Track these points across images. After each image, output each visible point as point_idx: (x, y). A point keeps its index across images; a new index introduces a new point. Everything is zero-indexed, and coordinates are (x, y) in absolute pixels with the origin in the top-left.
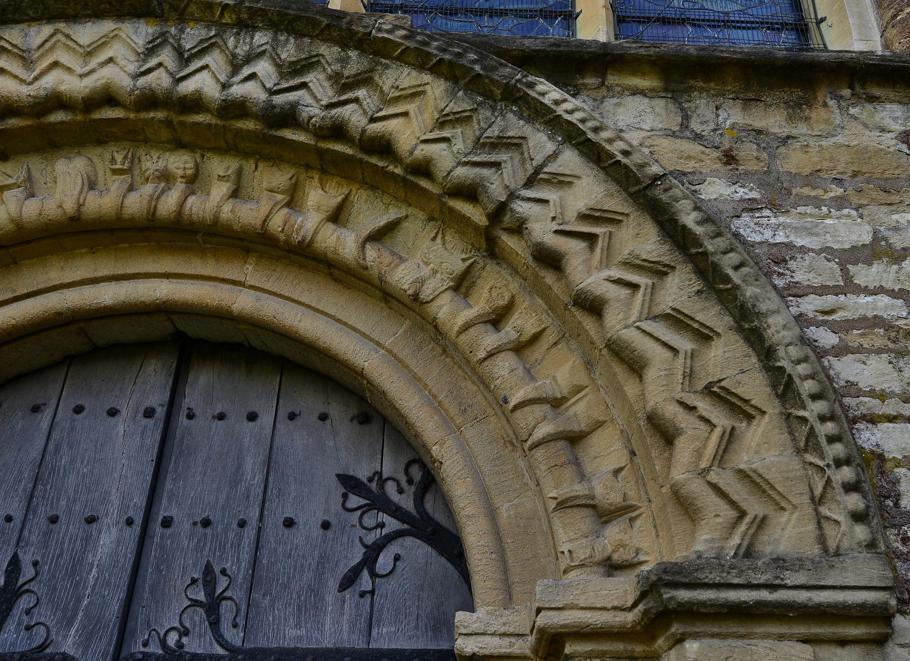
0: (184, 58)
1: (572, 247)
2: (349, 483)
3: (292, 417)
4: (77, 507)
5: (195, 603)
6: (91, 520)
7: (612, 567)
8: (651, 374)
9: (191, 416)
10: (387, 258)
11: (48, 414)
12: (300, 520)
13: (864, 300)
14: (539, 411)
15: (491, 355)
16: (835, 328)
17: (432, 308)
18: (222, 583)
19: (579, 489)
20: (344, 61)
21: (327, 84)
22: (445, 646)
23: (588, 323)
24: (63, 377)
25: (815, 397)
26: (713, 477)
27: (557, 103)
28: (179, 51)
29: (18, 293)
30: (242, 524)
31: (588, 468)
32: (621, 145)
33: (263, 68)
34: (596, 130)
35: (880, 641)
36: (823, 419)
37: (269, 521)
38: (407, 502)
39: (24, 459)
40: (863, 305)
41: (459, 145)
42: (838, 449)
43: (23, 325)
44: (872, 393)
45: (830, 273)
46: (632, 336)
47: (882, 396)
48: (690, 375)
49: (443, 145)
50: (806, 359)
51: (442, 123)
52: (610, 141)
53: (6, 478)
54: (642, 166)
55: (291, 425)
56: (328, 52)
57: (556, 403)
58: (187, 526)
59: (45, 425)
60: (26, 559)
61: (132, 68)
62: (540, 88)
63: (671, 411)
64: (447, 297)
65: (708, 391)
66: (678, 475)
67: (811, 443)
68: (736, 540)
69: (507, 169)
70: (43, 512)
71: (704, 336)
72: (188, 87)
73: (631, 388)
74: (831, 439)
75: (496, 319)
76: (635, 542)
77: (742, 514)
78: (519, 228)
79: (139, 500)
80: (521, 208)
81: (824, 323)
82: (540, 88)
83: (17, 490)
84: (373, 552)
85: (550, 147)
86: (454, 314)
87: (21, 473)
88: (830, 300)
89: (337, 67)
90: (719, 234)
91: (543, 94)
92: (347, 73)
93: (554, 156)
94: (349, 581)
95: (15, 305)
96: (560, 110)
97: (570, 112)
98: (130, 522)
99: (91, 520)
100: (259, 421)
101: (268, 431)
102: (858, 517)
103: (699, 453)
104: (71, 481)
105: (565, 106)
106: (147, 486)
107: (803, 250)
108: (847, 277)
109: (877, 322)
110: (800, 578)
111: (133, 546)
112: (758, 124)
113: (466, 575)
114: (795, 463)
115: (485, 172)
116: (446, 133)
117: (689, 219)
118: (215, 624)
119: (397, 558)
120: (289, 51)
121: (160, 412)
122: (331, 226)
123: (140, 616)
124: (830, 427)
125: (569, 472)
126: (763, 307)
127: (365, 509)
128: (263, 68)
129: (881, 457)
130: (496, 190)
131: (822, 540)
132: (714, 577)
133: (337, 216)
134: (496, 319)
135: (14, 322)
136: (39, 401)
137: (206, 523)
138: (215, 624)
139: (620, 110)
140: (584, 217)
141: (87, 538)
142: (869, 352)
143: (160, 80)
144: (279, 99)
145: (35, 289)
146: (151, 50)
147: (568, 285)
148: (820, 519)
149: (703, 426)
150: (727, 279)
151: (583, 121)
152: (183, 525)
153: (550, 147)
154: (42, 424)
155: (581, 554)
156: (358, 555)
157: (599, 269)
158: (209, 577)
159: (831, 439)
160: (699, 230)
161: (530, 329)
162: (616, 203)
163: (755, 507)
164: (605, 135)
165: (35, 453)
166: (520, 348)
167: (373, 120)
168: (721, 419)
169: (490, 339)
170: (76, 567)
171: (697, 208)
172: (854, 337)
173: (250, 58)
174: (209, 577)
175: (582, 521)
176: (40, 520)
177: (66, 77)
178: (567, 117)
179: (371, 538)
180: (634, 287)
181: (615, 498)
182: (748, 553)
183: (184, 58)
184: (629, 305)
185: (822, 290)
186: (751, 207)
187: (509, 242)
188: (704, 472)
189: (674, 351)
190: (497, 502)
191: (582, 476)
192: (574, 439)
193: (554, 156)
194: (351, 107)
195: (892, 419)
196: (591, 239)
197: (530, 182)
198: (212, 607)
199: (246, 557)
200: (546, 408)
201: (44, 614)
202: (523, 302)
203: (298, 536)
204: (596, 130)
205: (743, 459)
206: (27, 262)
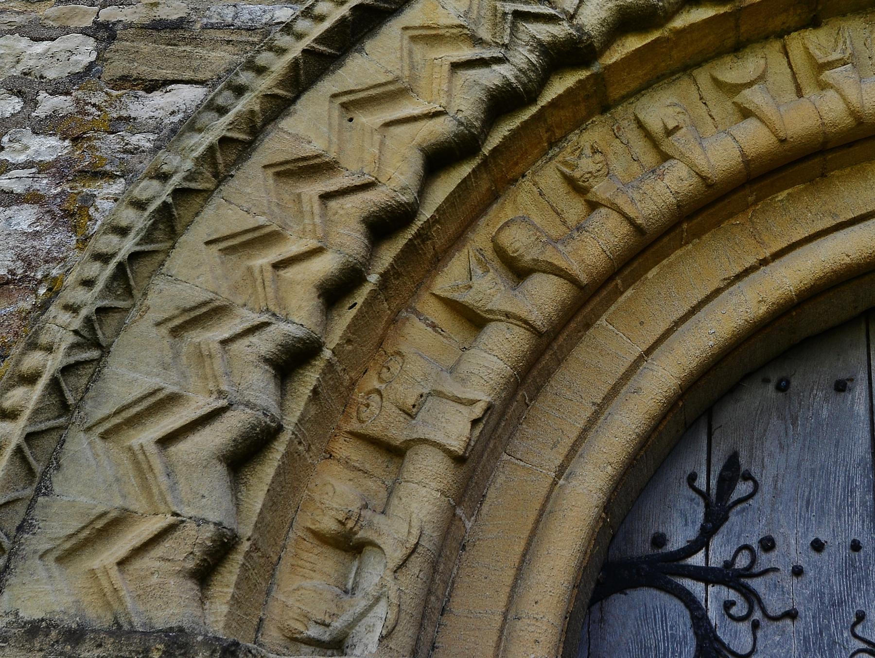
24: (864, 339)
29: (842, 219)
39: (847, 459)
43: (858, 265)
53: (831, 487)
83: (852, 505)
87: (849, 479)
95: (840, 235)
135: (848, 260)
136: (843, 375)
145: (864, 212)
154: (856, 408)
206: (837, 173)
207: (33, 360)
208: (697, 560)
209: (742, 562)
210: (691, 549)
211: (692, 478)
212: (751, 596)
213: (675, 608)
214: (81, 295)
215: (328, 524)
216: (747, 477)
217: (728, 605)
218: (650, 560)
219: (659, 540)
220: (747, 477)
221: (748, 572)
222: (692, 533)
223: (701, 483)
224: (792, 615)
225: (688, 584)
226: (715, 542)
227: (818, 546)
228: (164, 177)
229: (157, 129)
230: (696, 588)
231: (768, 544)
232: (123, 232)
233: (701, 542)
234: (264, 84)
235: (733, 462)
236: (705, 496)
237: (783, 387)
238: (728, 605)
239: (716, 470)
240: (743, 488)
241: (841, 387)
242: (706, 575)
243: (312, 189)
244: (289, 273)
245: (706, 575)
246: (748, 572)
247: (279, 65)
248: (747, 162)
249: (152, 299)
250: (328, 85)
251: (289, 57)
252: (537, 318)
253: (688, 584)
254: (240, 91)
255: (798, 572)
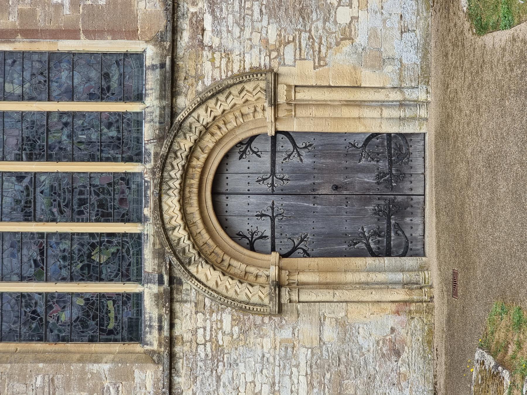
0: (170, 188)
1: (213, 114)
2: (240, 158)
3: (227, 170)
4: (246, 207)
5: (263, 183)
6: (248, 204)
7: (264, 110)
8: (237, 103)
9: (227, 190)
10: (207, 148)
11: (228, 217)
12: (248, 166)
13: (222, 66)
14: (238, 121)
15: (227, 129)
16: (228, 71)
17: (217, 140)
18: (260, 179)
19: (252, 115)
20: (171, 157)
21: (176, 161)
22: (270, 138)
23: (226, 112)
25: (243, 78)
26: (254, 95)
27: (183, 117)
28: (169, 189)
30: (249, 177)
31: (247, 113)
32: (193, 105)
33: (172, 173)
34: (190, 110)
35: (278, 74)
36: (246, 78)
37: (248, 172)
38: (244, 147)
40: (223, 66)
41: (191, 134)
42: (251, 76)
44: (240, 68)
45: (217, 71)
46: (230, 105)
47: (240, 66)
48: (237, 96)
49: (191, 137)
50: (236, 79)
51: (186, 138)
52: (192, 107)
54: (198, 102)
55: (229, 170)
56: (169, 161)
57: (236, 118)
58: (249, 186)
59: (230, 217)
60: (256, 214)
61: (174, 198)
62: (180, 119)
63: (244, 100)
64: (216, 137)
65: (239, 94)
66: (253, 100)
67: (250, 80)
68: (264, 92)
69: (196, 126)
70: (247, 213)
71: (230, 93)
72: (178, 186)
73: (238, 106)
74: (250, 77)
75: (219, 128)
76: (260, 106)
77: (260, 91)
78: (208, 123)
79: (245, 196)
80: (204, 123)
81: (227, 73)
82: (180, 119)
84: (254, 152)
85: (192, 118)
86: (219, 136)
88: (223, 71)
89: (173, 159)
90: (212, 89)
91: (181, 119)
92: (174, 156)
93: (193, 117)
94: (259, 156)
96: (185, 116)
97: (185, 114)
98: (249, 197)
99: (248, 204)
100: (228, 177)
101: (230, 174)
102: (261, 75)
103: (250, 96)
104: (240, 210)
105: (184, 115)
106: (242, 195)
107: (212, 74)
108: (217, 67)
109: (227, 65)
110: (270, 85)
111: (253, 195)
112: (183, 78)
113: (256, 136)
114: (252, 82)
115: (197, 129)
116: (188, 137)
117: (209, 94)
118: (267, 179)
119: (255, 148)
120: (169, 168)
121: (227, 196)
122: (199, 160)
123: (265, 192)
124: (248, 77)
125: (248, 116)
126: (227, 84)
127: (246, 154)
128: (172, 173)
129: (250, 68)
130: (201, 128)
131: (264, 80)
132: (270, 97)
133: (198, 159)
134: (219, 128)
137: (249, 183)
138: (267, 179)
139: (180, 104)
140: (206, 112)
141: (252, 204)
142: (232, 67)
143: (176, 192)
144: (181, 168)
146: (168, 195)
147: (220, 115)
148: (261, 80)
149: (246, 95)
150: (221, 89)
151: (188, 112)
152: (249, 187)
153: (192, 118)
155: (262, 114)
156: (254, 155)
157: (217, 110)
158: (258, 181)
159: (250, 77)
160: (212, 93)
161: (223, 122)
162: (204, 107)
163: (258, 89)
164: (191, 108)
165: (235, 217)
166: (225, 124)
167: (186, 151)
168: (244, 92)
169: (224, 129)
170: (257, 205)
171: (207, 93)
172: (230, 69)
173: (170, 176)
174: (258, 181)
175: (256, 114)
176: (249, 214)
177: (176, 209)
178: (187, 114)
179: (251, 153)
180: (221, 104)
181: (253, 109)
182: (265, 91)
183: (170, 188)
184: (224, 105)
185: (220, 72)
186: (203, 83)
187: (209, 125)
188: (253, 96)
189: (233, 98)
190: (250, 128)
191: (249, 114)
192: (242, 115)
193: (193, 117)
194: (182, 155)
195: (244, 65)
196: (211, 111)
197: (198, 121)
198: (264, 180)
199: (255, 175)
200: (237, 120)
201: (265, 209)
202: (217, 123)
203: (251, 166)
204: (190, 110)
205: (251, 90)
207: (244, 307)
208: (250, 239)
209: (250, 233)
210: (249, 240)
211: (239, 240)
212: (254, 233)
213: (256, 242)
214: (236, 304)
215: (255, 279)
216: (239, 232)
217: (256, 235)
218: (250, 245)
219: (248, 244)
220: (239, 232)
221: (252, 233)
222: (247, 240)
223: (240, 238)
224: (257, 227)
225: (253, 240)
226: (248, 237)
227: (248, 224)
228: (221, 298)
229: (211, 303)
230: (254, 239)
231: (248, 230)
232: (228, 301)
233: (248, 238)
234: (207, 289)
235: (237, 234)
236: (242, 238)
237: (226, 227)
238: (256, 235)
239: (238, 236)
240: (241, 233)
241: (227, 220)
242: (252, 238)
243: (219, 282)
244: (231, 284)
245: (252, 238)
246: (252, 233)
247: (205, 288)
248: (207, 232)
249: (235, 298)
250: (205, 283)
251: (204, 287)
252: (229, 258)
253: (253, 240)
254: (208, 292)
255: (252, 226)
